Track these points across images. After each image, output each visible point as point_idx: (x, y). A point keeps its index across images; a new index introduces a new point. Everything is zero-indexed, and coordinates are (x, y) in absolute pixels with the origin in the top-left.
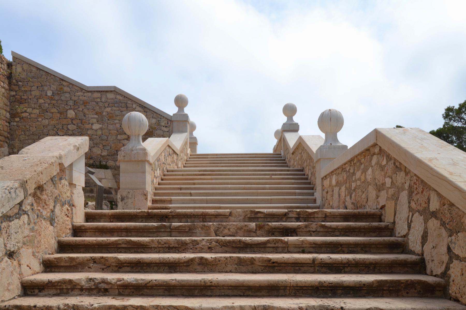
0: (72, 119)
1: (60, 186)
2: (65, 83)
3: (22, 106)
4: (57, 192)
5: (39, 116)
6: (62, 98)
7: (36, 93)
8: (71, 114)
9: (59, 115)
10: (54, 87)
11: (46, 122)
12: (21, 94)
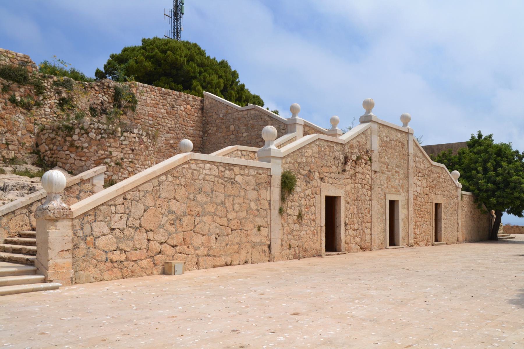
0: (233, 131)
1: (84, 186)
2: (229, 108)
3: (208, 126)
4: (81, 188)
5: (217, 131)
6: (228, 118)
7: (215, 117)
8: (232, 127)
9: (226, 129)
10: (224, 111)
11: (220, 135)
12: (208, 118)
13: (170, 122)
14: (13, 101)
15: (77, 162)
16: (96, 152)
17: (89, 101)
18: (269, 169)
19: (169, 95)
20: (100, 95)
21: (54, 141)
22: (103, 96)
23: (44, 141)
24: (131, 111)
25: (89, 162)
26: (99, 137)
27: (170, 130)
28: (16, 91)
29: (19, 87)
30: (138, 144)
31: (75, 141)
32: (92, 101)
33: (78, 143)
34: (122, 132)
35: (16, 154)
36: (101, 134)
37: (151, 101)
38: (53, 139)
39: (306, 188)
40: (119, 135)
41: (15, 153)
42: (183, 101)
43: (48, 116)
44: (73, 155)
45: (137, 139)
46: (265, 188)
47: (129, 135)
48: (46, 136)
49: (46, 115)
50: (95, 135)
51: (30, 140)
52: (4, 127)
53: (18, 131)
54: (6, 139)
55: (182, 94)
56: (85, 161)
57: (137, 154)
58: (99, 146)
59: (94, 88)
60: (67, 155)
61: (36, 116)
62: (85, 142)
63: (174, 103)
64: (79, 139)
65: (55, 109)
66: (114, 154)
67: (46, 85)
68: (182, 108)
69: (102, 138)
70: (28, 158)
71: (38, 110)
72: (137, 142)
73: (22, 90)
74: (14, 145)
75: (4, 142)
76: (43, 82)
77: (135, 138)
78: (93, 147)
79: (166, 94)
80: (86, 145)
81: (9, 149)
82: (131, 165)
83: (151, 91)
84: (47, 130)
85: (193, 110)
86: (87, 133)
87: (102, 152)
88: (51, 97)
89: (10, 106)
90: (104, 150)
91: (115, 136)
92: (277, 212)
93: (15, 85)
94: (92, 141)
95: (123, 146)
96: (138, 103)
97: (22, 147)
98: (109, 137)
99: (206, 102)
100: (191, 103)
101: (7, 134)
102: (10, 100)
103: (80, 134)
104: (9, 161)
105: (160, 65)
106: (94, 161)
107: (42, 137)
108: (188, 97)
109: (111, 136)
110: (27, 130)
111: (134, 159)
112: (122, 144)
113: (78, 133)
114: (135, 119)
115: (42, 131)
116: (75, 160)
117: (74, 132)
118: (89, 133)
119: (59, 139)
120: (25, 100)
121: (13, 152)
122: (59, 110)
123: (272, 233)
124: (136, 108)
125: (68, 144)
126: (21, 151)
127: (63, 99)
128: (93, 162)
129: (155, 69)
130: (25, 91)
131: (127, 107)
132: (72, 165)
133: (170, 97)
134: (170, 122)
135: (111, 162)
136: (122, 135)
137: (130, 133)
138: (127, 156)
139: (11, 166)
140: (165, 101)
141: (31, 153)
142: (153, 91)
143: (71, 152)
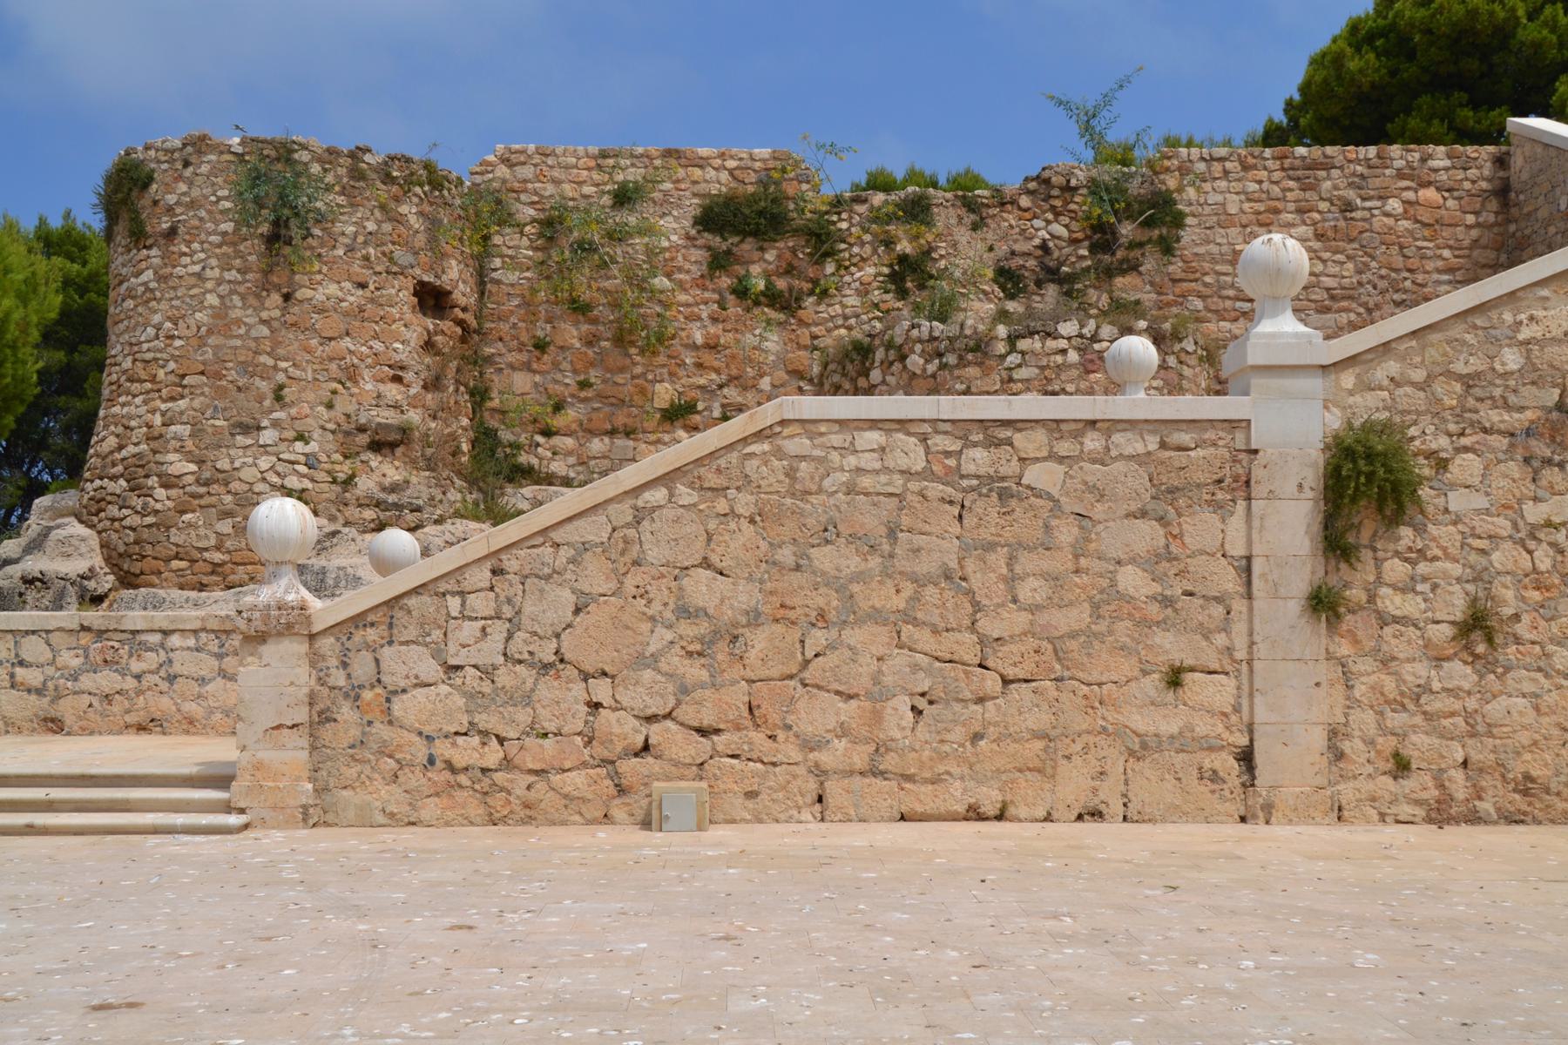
7: (1543, 213)
13: (1334, 269)
14: (741, 292)
17: (991, 249)
18: (1232, 424)
19: (1328, 167)
20: (1038, 223)
22: (1048, 222)
24: (1158, 255)
27: (1333, 298)
28: (754, 262)
29: (762, 249)
30: (1075, 373)
32: (1002, 249)
34: (1012, 340)
36: (940, 355)
37: (1246, 206)
39: (1529, 488)
40: (1001, 348)
42: (1400, 175)
43: (853, 321)
45: (1073, 356)
46: (1217, 506)
47: (1038, 345)
49: (846, 318)
50: (922, 361)
52: (718, 371)
54: (723, 406)
55: (1395, 150)
59: (1013, 202)
61: (817, 325)
63: (1351, 194)
65: (876, 295)
67: (844, 225)
68: (1394, 205)
69: (943, 367)
71: (822, 308)
72: (1071, 366)
73: (770, 256)
76: (835, 218)
77: (1064, 352)
79: (1314, 166)
83: (1246, 168)
85: (1451, 203)
86: (903, 358)
88: (863, 260)
89: (734, 309)
91: (986, 354)
92: (1294, 607)
93: (748, 245)
96: (1189, 221)
98: (962, 363)
99: (1517, 161)
100: (1443, 176)
101: (725, 390)
102: (734, 291)
105: (1411, 56)
108: (1423, 160)
109: (970, 357)
110: (788, 372)
112: (1011, 380)
114: (1174, 281)
120: (781, 284)
122: (889, 297)
123: (1258, 699)
124: (1178, 240)
127: (903, 259)
129: (1393, 73)
130: (779, 257)
131: (1141, 245)
133: (1335, 173)
134: (1334, 269)
136: (1012, 349)
137: (1043, 340)
140: (1308, 195)
142: (1254, 167)
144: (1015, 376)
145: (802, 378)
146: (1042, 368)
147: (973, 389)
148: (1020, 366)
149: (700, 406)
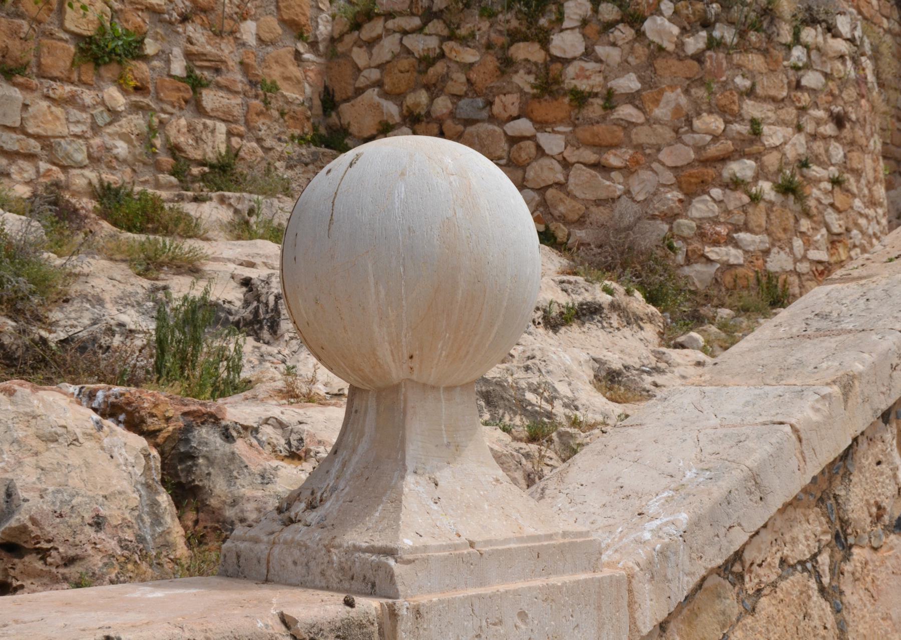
15: (580, 178)
16: (684, 122)
21: (439, 68)
23: (375, 74)
25: (645, 175)
26: (695, 43)
31: (566, 62)
33: (583, 75)
35: (235, 141)
36: (707, 25)
38: (427, 62)
40: (785, 34)
41: (230, 134)
44: (553, 143)
47: (820, 39)
48: (388, 46)
50: (676, 30)
51: (294, 71)
53: (243, 18)
54: (189, 55)
56: (627, 171)
57: (852, 143)
58: (700, 93)
60: (514, 140)
62: (624, 67)
64: (589, 54)
66: (773, 135)
69: (713, 44)
70: (290, 167)
74: (228, 89)
75: (178, 67)
77: (842, 57)
78: (669, 95)
80: (629, 83)
81: (200, 110)
82: (839, 199)
84: (389, 15)
87: (715, 123)
90: (729, 114)
91: (769, 38)
94: (660, 63)
95: (805, 98)
97: (266, 103)
98: (743, 46)
101: (190, 27)
103: (593, 27)
104: (203, 177)
106: (675, 169)
107: (360, 56)
109: (753, 37)
111: (845, 166)
112: (798, 86)
113: (585, 22)
115: (356, 26)
116: (566, 165)
117: (560, 19)
118: (644, 19)
119: (470, 56)
121: (222, 128)
125: (523, 80)
126: (260, 122)
128: (669, 177)
132: (550, 193)
135: (756, 178)
137: (824, 34)
138: (818, 147)
139: (222, 200)
141: (302, 140)
143: (542, 125)
144: (804, 82)
145: (300, 37)
146: (826, 75)
147: (759, 90)
148: (808, 66)
149: (150, 47)
